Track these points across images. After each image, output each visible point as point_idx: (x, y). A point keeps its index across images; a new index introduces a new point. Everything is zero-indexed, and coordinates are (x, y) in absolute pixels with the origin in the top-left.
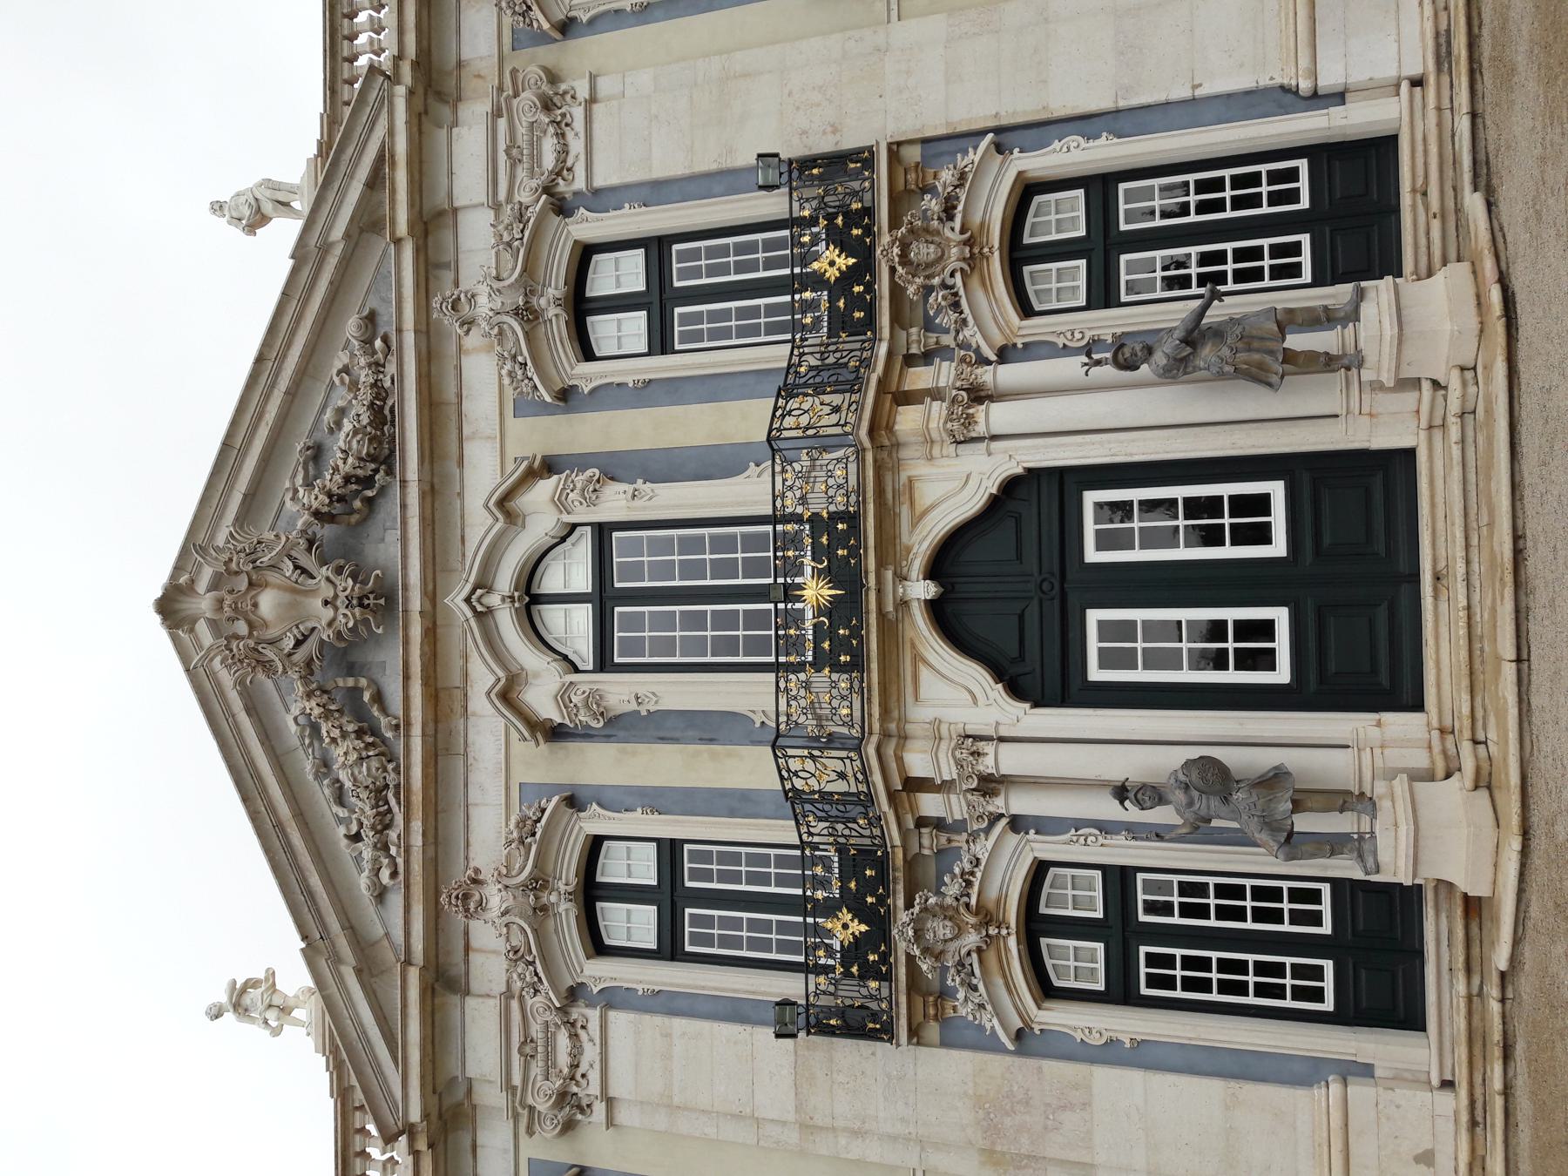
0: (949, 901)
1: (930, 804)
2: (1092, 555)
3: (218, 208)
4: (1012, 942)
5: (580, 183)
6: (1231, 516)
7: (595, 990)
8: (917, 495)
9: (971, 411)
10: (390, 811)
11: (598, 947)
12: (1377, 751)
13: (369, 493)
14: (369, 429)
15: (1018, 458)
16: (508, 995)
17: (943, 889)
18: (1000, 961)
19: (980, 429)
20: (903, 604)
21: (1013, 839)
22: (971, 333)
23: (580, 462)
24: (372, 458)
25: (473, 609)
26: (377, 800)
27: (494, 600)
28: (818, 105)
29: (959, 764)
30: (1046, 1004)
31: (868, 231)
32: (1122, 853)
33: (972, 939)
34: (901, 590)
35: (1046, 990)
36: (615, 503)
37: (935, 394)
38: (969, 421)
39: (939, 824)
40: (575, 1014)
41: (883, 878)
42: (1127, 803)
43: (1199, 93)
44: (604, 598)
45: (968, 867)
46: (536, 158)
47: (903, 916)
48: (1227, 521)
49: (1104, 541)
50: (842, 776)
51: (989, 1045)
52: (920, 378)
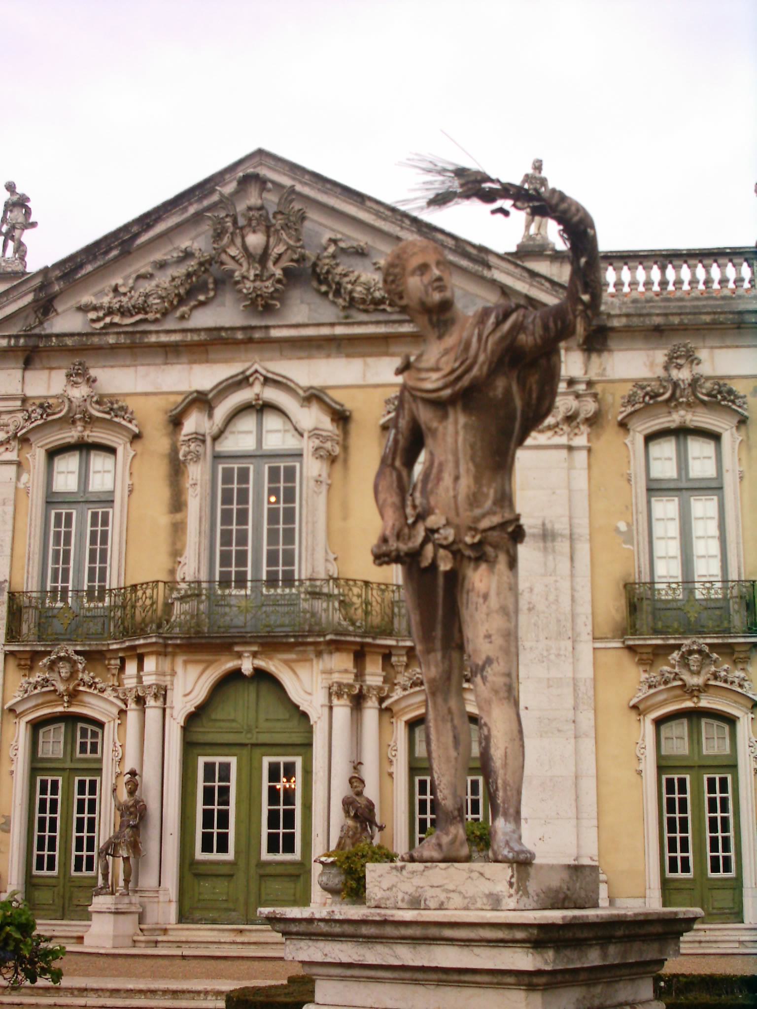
0: (80, 675)
3: (538, 166)
4: (60, 709)
6: (284, 833)
7: (28, 456)
8: (302, 664)
9: (345, 696)
10: (132, 316)
11: (53, 454)
12: (156, 900)
13: (331, 296)
14: (370, 297)
15: (319, 722)
16: (25, 400)
17: (87, 672)
18: (52, 701)
19: (335, 701)
20: (239, 655)
21: (115, 711)
22: (398, 693)
24: (352, 299)
25: (251, 375)
26: (139, 309)
27: (257, 388)
28: (547, 599)
29: (150, 686)
30: (29, 726)
33: (61, 687)
34: (246, 655)
35: (36, 726)
37: (360, 675)
38: (339, 695)
39: (122, 668)
40: (14, 444)
42: (129, 776)
43: (523, 822)
45: (99, 686)
47: (71, 649)
48: (281, 831)
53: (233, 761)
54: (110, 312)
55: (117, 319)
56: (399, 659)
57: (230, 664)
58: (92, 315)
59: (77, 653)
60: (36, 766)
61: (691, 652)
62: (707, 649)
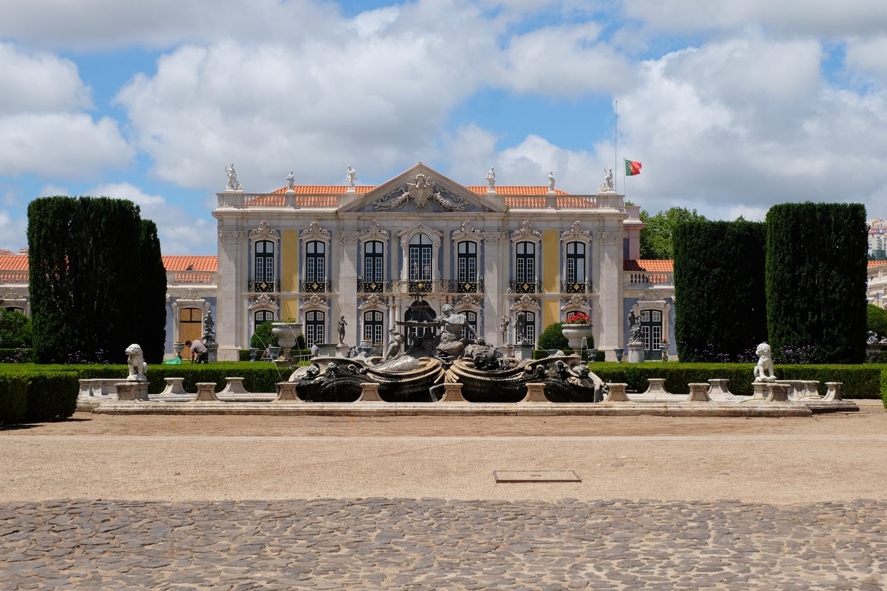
1: (391, 299)
23: (442, 243)
36: (435, 250)
39: (388, 299)
51: (358, 307)
52: (450, 298)
55: (383, 208)
58: (376, 207)
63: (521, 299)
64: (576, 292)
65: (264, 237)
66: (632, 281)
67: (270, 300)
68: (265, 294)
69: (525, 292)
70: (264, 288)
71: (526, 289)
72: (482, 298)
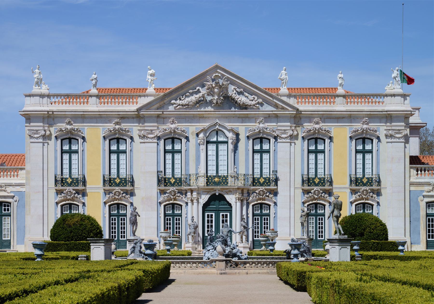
2: (221, 214)
5: (279, 140)
25: (216, 123)
31: (265, 185)
32: (184, 216)
41: (179, 185)
44: (217, 143)
46: (283, 133)
49: (223, 215)
50: (193, 183)
53: (214, 214)
54: (179, 105)
55: (181, 107)
56: (251, 192)
57: (213, 193)
58: (174, 106)
59: (176, 189)
60: (165, 215)
61: (316, 191)
62: (319, 190)
63: (312, 191)
64: (364, 185)
65: (69, 134)
66: (417, 174)
67: (75, 194)
68: (71, 188)
69: (317, 185)
70: (69, 182)
71: (317, 182)
72: (275, 191)
